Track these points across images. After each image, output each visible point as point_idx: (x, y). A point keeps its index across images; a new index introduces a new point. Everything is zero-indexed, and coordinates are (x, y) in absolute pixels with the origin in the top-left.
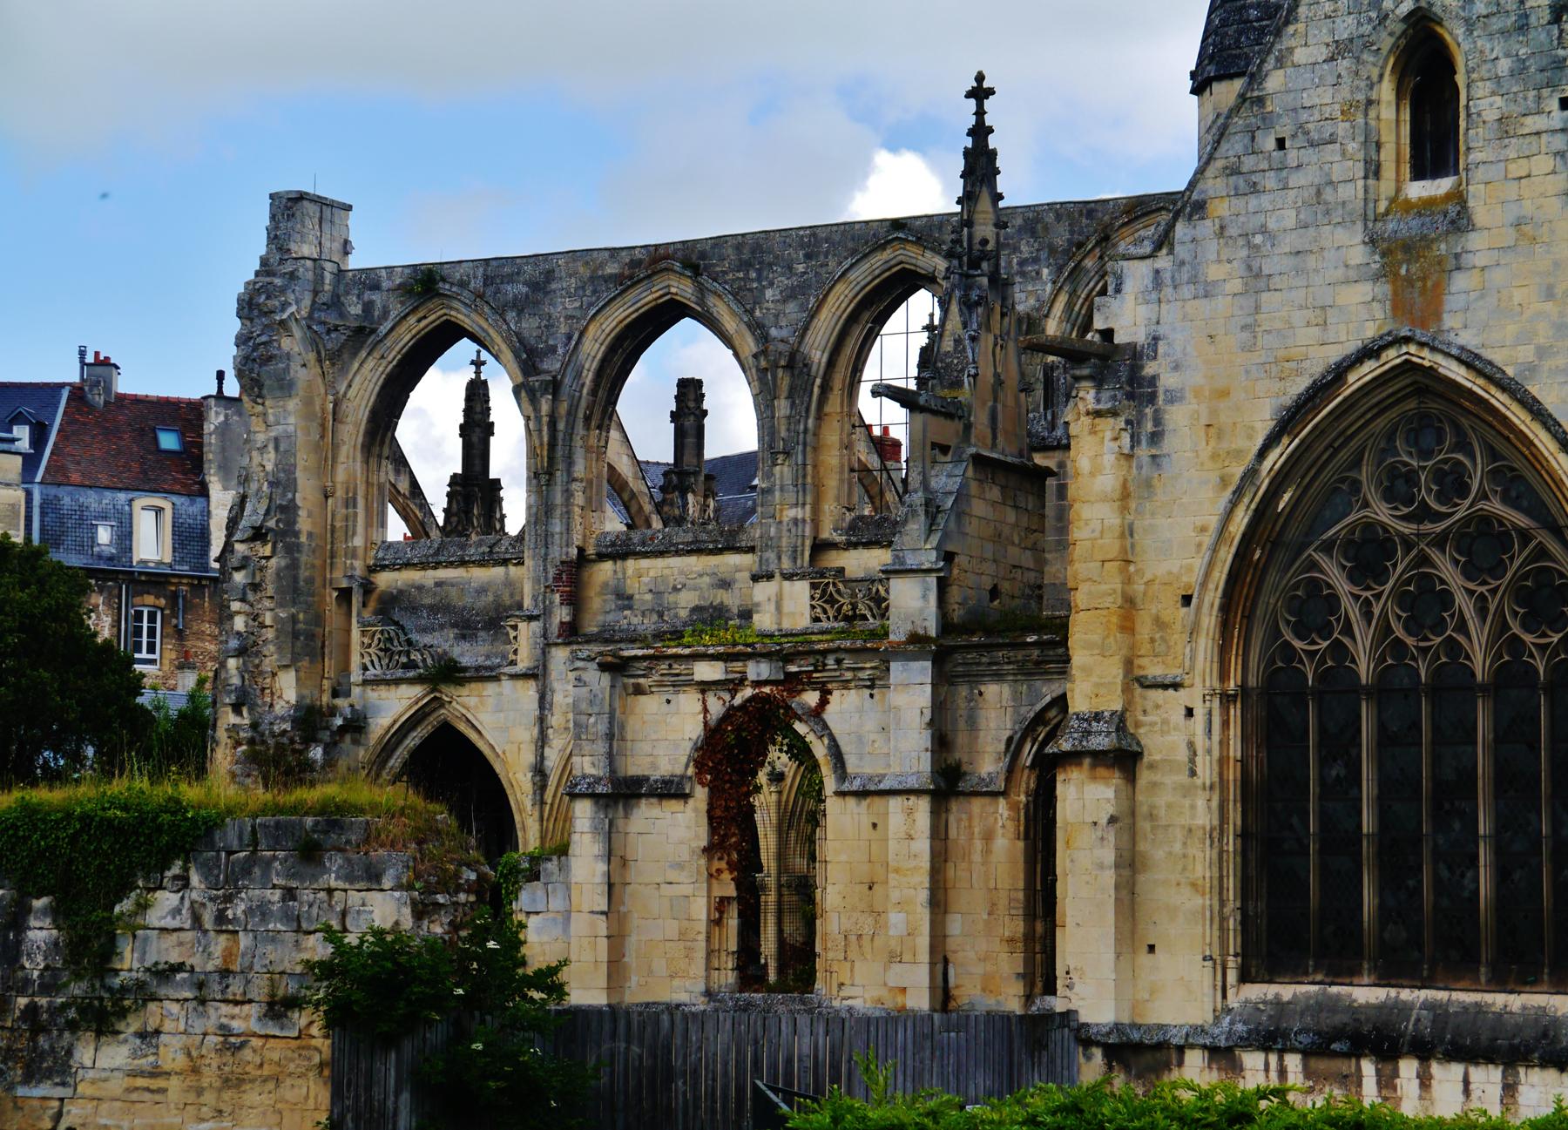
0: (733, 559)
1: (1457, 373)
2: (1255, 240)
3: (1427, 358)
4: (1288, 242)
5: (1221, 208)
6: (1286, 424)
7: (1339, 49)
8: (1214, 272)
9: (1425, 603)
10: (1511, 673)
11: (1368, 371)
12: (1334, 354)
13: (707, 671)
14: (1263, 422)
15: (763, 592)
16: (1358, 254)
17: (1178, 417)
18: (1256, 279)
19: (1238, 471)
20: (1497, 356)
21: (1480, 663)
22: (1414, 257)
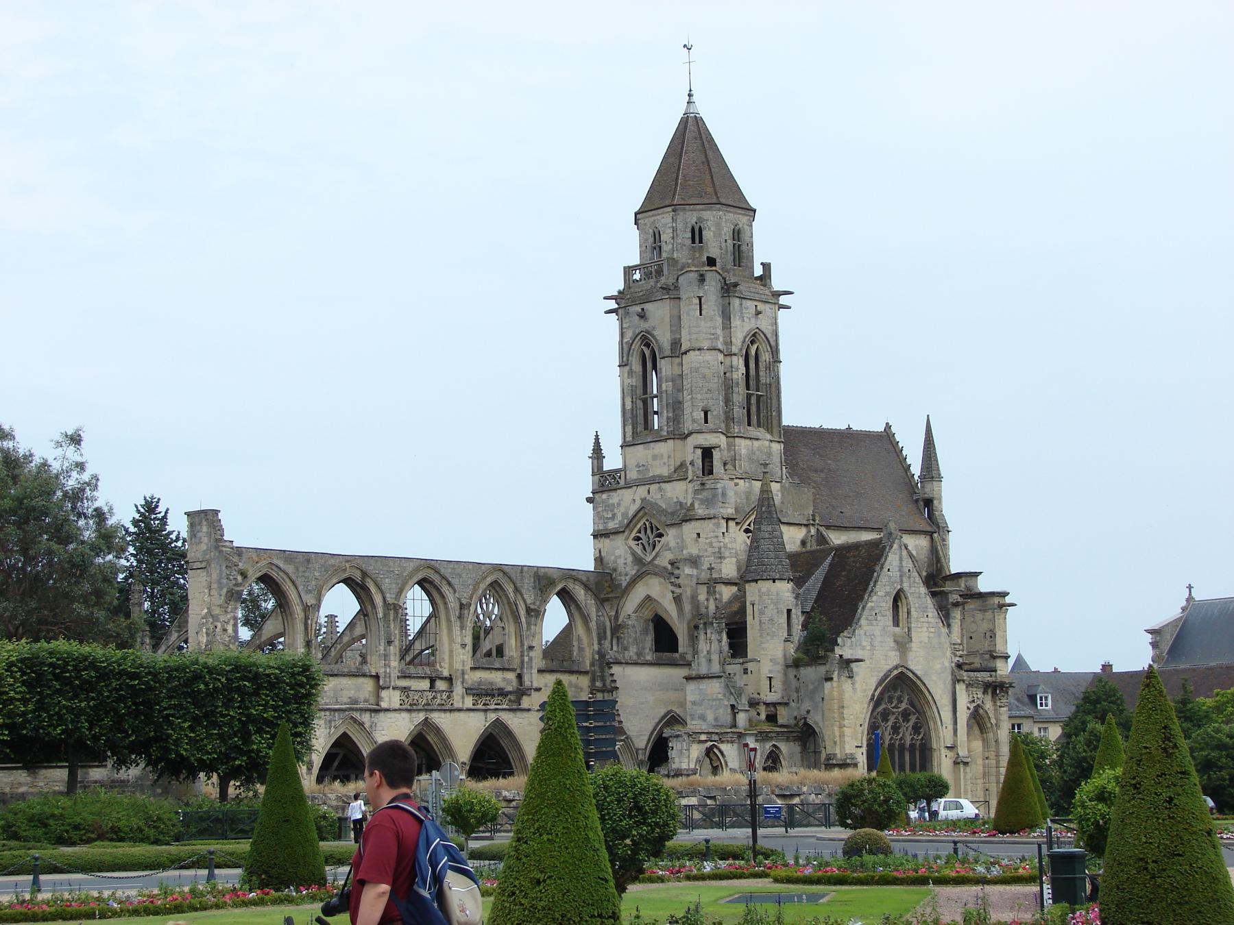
0: (361, 680)
1: (911, 675)
2: (872, 637)
3: (905, 671)
4: (879, 639)
5: (865, 628)
6: (879, 684)
7: (887, 594)
8: (864, 644)
9: (896, 729)
10: (912, 745)
11: (896, 672)
12: (888, 668)
13: (703, 737)
14: (873, 681)
15: (384, 694)
16: (892, 644)
17: (857, 678)
18: (872, 645)
19: (870, 693)
20: (918, 673)
21: (908, 743)
22: (902, 645)
